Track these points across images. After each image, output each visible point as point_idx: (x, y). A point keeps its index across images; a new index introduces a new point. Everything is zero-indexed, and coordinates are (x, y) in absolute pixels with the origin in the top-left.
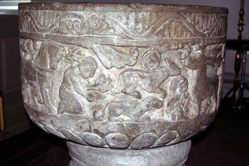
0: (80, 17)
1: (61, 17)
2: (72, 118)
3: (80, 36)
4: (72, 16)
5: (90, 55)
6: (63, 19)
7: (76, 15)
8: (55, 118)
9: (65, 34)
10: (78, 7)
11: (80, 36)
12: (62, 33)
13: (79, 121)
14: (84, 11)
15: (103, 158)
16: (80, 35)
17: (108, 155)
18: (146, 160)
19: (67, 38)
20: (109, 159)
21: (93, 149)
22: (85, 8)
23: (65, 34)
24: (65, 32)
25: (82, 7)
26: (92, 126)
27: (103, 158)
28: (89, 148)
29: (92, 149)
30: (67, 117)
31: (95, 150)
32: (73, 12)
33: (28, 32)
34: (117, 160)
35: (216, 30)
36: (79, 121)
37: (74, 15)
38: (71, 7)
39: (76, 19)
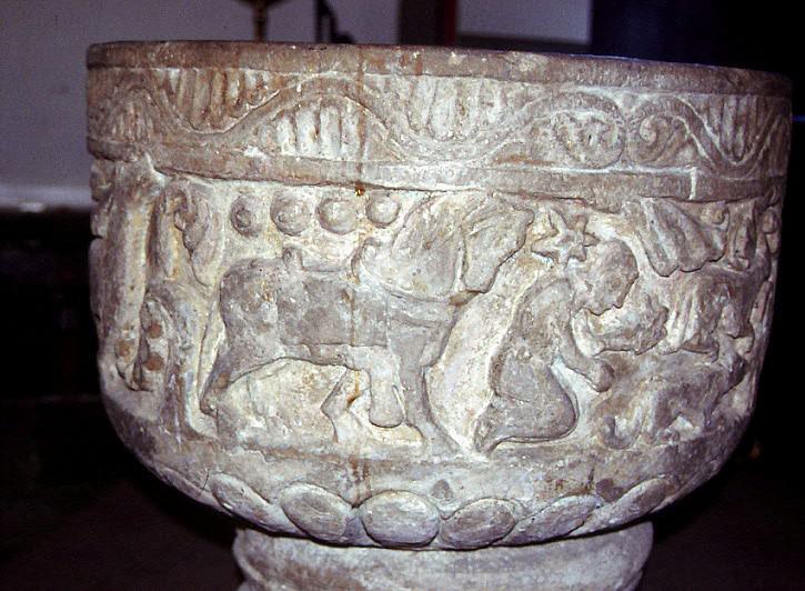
0: (608, 106)
1: (538, 104)
2: (533, 456)
3: (599, 171)
4: (581, 103)
5: (614, 235)
6: (546, 112)
7: (593, 101)
8: (463, 470)
9: (549, 164)
10: (602, 72)
11: (599, 171)
12: (539, 162)
13: (561, 463)
14: (620, 85)
15: (519, 579)
16: (599, 168)
17: (530, 564)
18: (625, 553)
19: (555, 179)
20: (538, 577)
21: (469, 560)
22: (625, 79)
23: (549, 164)
24: (548, 159)
25: (615, 74)
26: (597, 470)
27: (519, 579)
28: (454, 560)
29: (466, 559)
30: (514, 459)
31: (480, 561)
32: (581, 88)
33: (329, 153)
34: (563, 575)
35: (773, 139)
36: (561, 463)
37: (589, 101)
38: (581, 71)
39: (592, 113)
